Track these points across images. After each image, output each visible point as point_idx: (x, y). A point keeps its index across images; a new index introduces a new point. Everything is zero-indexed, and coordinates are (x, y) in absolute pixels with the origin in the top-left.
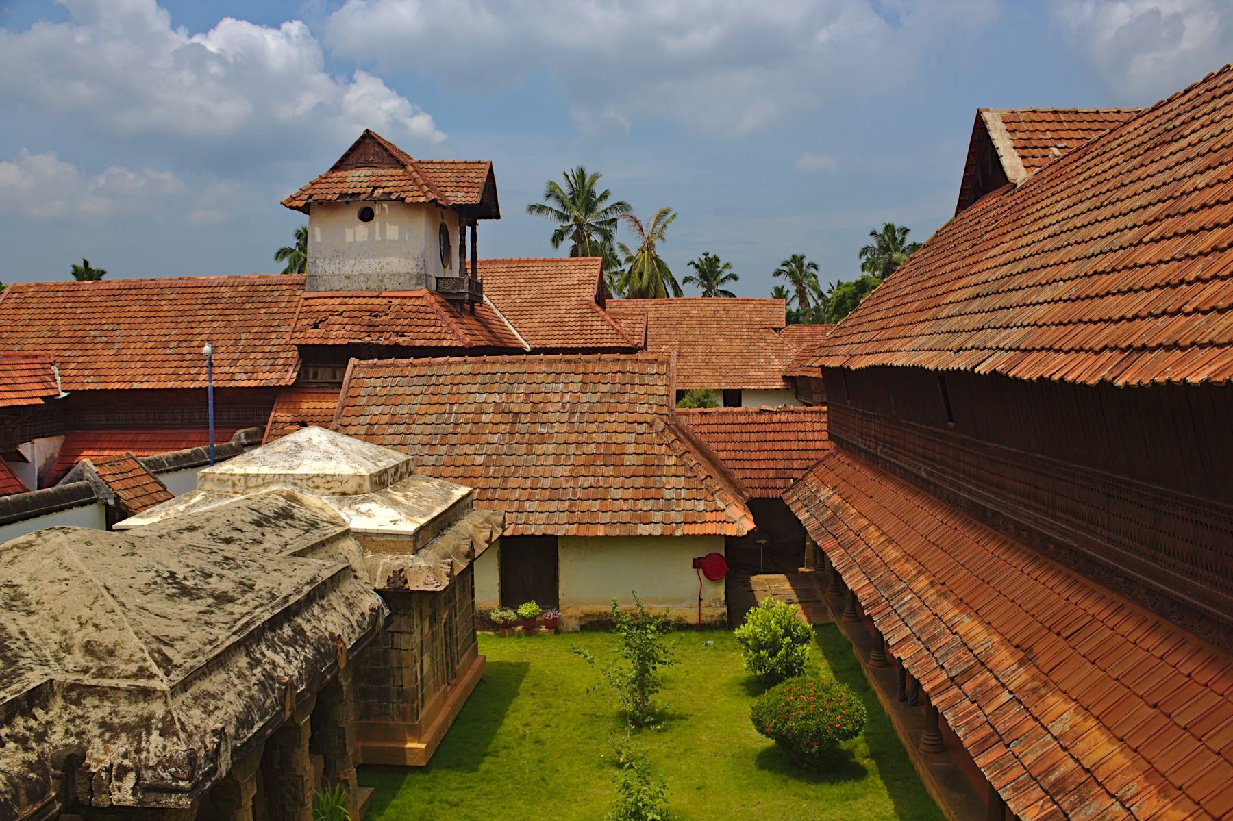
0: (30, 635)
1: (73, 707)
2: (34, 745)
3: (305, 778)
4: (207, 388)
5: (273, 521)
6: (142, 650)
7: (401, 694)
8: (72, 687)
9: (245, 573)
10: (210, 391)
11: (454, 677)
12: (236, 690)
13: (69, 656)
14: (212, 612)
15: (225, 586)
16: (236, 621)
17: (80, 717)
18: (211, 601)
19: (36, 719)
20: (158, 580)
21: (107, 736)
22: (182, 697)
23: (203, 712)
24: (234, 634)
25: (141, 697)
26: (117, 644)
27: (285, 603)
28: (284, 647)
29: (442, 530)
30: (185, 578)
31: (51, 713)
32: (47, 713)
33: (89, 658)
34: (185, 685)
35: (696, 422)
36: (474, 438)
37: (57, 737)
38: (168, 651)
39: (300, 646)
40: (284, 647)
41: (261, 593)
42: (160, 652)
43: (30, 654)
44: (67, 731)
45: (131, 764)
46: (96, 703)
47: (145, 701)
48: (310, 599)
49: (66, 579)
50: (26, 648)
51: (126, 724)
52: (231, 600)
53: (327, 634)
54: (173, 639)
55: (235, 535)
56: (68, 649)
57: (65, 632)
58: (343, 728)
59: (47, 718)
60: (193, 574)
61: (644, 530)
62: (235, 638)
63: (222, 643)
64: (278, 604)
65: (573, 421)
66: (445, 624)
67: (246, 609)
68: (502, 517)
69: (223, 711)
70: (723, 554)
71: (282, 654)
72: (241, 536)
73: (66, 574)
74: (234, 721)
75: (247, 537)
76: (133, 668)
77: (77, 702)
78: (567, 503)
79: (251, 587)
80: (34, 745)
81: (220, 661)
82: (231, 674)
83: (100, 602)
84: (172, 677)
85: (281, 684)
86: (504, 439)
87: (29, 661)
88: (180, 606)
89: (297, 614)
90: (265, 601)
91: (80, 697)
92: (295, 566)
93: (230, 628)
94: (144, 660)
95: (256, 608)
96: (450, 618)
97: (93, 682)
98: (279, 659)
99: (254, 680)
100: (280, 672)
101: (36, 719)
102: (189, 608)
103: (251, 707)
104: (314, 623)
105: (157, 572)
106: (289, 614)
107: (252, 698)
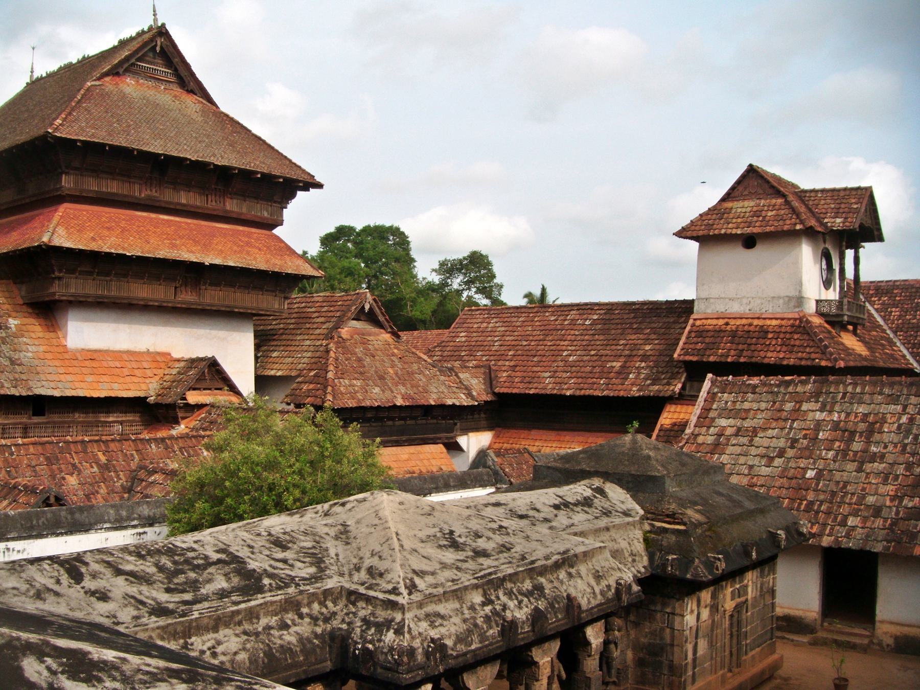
0: (341, 557)
1: (351, 606)
5: (571, 506)
6: (399, 577)
9: (507, 539)
11: (739, 665)
13: (357, 574)
14: (466, 561)
15: (489, 546)
16: (480, 571)
18: (472, 554)
19: (327, 608)
20: (439, 535)
21: (364, 627)
23: (429, 625)
24: (475, 578)
25: (389, 606)
26: (387, 571)
28: (520, 597)
30: (460, 536)
31: (338, 607)
33: (368, 576)
34: (420, 605)
36: (807, 453)
38: (417, 580)
39: (535, 598)
41: (515, 554)
42: (411, 580)
46: (364, 606)
48: (557, 566)
49: (376, 525)
51: (377, 622)
53: (565, 595)
57: (361, 558)
59: (335, 609)
60: (468, 534)
62: (476, 581)
63: (462, 583)
65: (906, 441)
67: (495, 563)
69: (446, 628)
71: (516, 602)
73: (376, 521)
74: (453, 638)
76: (390, 587)
77: (354, 604)
79: (509, 549)
80: (321, 623)
81: (456, 595)
84: (412, 597)
87: (333, 572)
89: (541, 574)
90: (514, 561)
92: (556, 540)
93: (474, 574)
94: (399, 583)
95: (503, 564)
98: (512, 604)
99: (482, 613)
100: (508, 615)
101: (327, 608)
102: (450, 556)
103: (472, 631)
104: (556, 584)
105: (441, 529)
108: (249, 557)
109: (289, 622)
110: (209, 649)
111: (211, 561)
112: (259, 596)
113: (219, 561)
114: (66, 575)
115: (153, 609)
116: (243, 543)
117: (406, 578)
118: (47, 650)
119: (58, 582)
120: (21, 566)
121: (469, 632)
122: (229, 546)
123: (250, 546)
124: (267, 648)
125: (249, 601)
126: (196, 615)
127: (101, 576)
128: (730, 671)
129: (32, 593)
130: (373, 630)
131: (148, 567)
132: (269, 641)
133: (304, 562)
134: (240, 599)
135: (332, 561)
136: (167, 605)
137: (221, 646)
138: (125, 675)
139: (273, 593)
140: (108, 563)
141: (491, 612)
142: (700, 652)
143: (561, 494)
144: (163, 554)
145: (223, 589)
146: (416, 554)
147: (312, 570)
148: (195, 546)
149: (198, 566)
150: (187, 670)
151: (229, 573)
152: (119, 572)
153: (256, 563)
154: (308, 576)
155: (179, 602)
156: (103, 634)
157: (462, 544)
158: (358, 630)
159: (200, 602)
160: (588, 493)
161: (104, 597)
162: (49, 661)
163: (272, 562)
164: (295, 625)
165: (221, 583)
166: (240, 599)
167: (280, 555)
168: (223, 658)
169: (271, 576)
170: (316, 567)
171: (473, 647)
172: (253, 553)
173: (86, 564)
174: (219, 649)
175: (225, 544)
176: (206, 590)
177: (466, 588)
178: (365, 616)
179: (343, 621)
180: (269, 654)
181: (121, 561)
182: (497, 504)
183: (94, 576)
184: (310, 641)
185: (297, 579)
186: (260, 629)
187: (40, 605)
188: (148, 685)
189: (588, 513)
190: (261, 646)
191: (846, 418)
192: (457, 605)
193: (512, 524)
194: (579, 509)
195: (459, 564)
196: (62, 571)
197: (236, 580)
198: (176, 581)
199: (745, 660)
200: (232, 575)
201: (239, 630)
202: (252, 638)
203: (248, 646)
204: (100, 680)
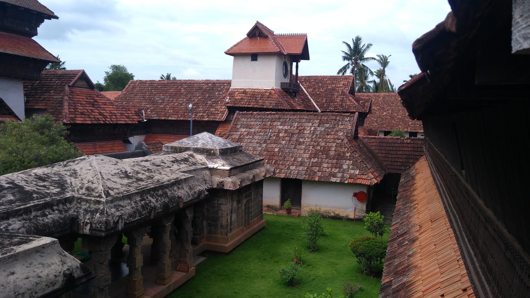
0: (73, 184)
1: (78, 204)
2: (64, 213)
3: (167, 244)
4: (190, 120)
6: (102, 190)
7: (222, 226)
8: (80, 198)
10: (191, 122)
11: (248, 224)
13: (81, 190)
14: (133, 183)
15: (143, 177)
16: (139, 187)
17: (79, 207)
19: (66, 206)
20: (120, 173)
22: (109, 205)
24: (136, 190)
25: (97, 203)
26: (96, 188)
27: (162, 184)
28: (157, 197)
29: (245, 171)
30: (130, 173)
31: (72, 205)
32: (70, 205)
34: (112, 202)
35: (371, 141)
36: (275, 142)
37: (71, 212)
38: (110, 191)
40: (157, 197)
41: (155, 180)
42: (108, 191)
43: (71, 188)
45: (89, 222)
46: (85, 204)
47: (98, 205)
50: (70, 187)
54: (114, 188)
57: (83, 184)
58: (188, 231)
60: (133, 172)
61: (333, 180)
63: (131, 192)
64: (158, 184)
65: (313, 137)
66: (245, 205)
68: (273, 169)
69: (124, 211)
70: (366, 192)
71: (155, 199)
73: (91, 168)
74: (127, 215)
76: (97, 195)
77: (80, 203)
78: (306, 168)
79: (152, 178)
80: (64, 213)
82: (132, 201)
83: (96, 176)
85: (151, 207)
86: (287, 143)
87: (69, 190)
88: (123, 180)
91: (81, 202)
93: (137, 188)
95: (149, 184)
96: (248, 202)
97: (85, 198)
98: (153, 200)
101: (66, 206)
102: (126, 181)
103: (136, 212)
104: (173, 192)
107: (137, 210)
108: (25, 185)
109: (47, 213)
110: (4, 228)
116: (21, 179)
117: (106, 191)
121: (135, 212)
124: (36, 226)
128: (245, 227)
132: (37, 222)
133: (54, 187)
139: (38, 201)
141: (144, 203)
142: (233, 219)
143: (175, 157)
145: (11, 200)
146: (110, 181)
151: (15, 192)
154: (56, 192)
157: (131, 176)
160: (187, 156)
163: (38, 187)
164: (50, 214)
170: (60, 188)
171: (136, 219)
172: (27, 183)
174: (10, 228)
175: (12, 180)
178: (85, 208)
179: (75, 211)
182: (147, 161)
189: (187, 164)
191: (290, 128)
192: (129, 202)
197: (18, 196)
199: (251, 222)
200: (16, 193)
202: (28, 221)
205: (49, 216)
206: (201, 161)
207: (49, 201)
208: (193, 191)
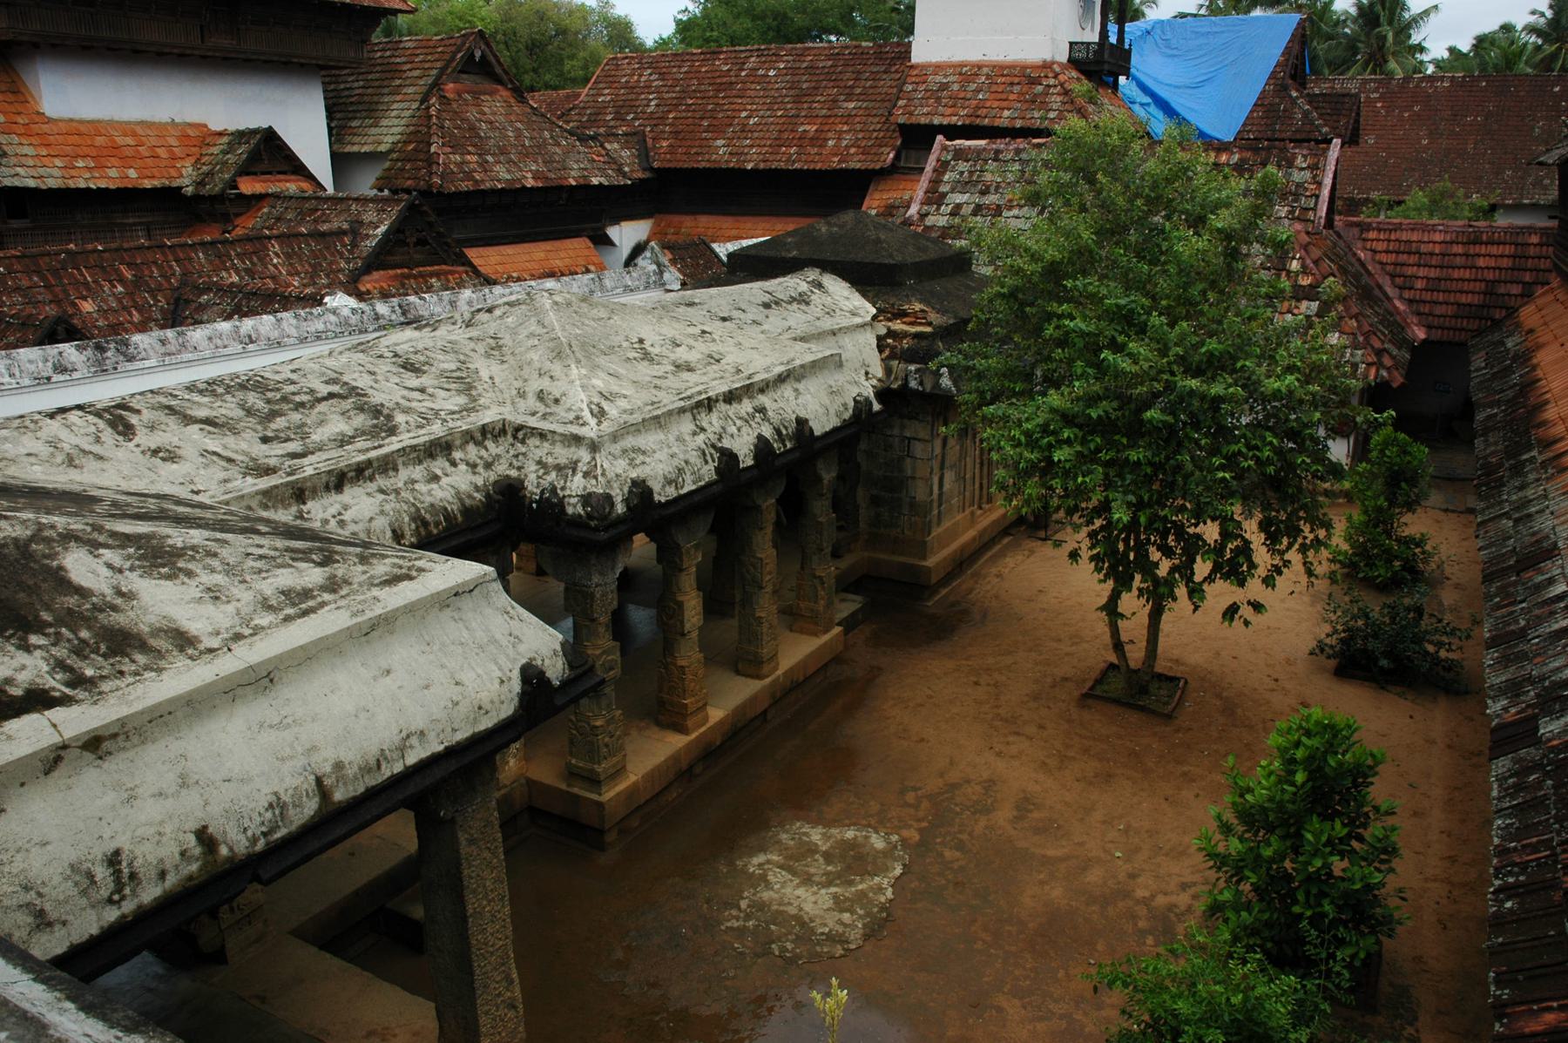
0: (497, 380)
7: (913, 505)
12: (670, 452)
19: (487, 450)
20: (625, 344)
21: (542, 471)
28: (739, 423)
31: (501, 448)
34: (615, 437)
37: (502, 469)
38: (606, 405)
42: (598, 405)
44: (511, 464)
46: (538, 443)
52: (690, 370)
55: (736, 314)
56: (522, 394)
57: (526, 381)
62: (682, 403)
67: (705, 379)
72: (742, 316)
75: (750, 317)
76: (571, 416)
77: (523, 442)
79: (718, 361)
84: (601, 427)
89: (762, 391)
90: (727, 375)
94: (582, 410)
99: (692, 445)
101: (487, 450)
102: (645, 371)
106: (748, 390)
107: (687, 462)
109: (439, 472)
111: (319, 395)
112: (394, 439)
113: (331, 396)
114: (109, 430)
115: (247, 468)
118: (102, 539)
119: (98, 440)
120: (36, 422)
121: (680, 471)
122: (341, 374)
123: (372, 373)
125: (380, 446)
126: (309, 471)
127: (163, 427)
128: (980, 508)
129: (59, 459)
130: (554, 474)
131: (228, 408)
133: (448, 390)
134: (369, 444)
135: (486, 386)
136: (266, 460)
137: (349, 512)
138: (228, 564)
139: (412, 435)
140: (169, 408)
142: (947, 486)
143: (770, 290)
144: (247, 388)
147: (462, 400)
148: (294, 377)
149: (302, 405)
150: (321, 550)
152: (188, 420)
153: (383, 396)
154: (456, 408)
155: (282, 456)
156: (181, 509)
158: (532, 477)
159: (313, 453)
160: (804, 287)
161: (171, 456)
162: (107, 554)
163: (405, 393)
164: (447, 475)
165: (338, 426)
166: (369, 444)
167: (414, 382)
168: (352, 528)
169: (407, 411)
172: (376, 381)
173: (138, 412)
174: (347, 516)
176: (316, 437)
177: (670, 413)
180: (417, 518)
181: (188, 405)
183: (152, 428)
184: (470, 496)
185: (442, 413)
186: (400, 485)
187: (74, 475)
188: (264, 575)
190: (406, 508)
193: (716, 328)
194: (795, 306)
195: (658, 382)
196: (101, 424)
197: (360, 420)
198: (273, 426)
200: (352, 413)
201: (372, 487)
203: (387, 507)
204: (190, 574)
205: (445, 481)
206: (847, 303)
207: (442, 434)
208: (839, 401)
